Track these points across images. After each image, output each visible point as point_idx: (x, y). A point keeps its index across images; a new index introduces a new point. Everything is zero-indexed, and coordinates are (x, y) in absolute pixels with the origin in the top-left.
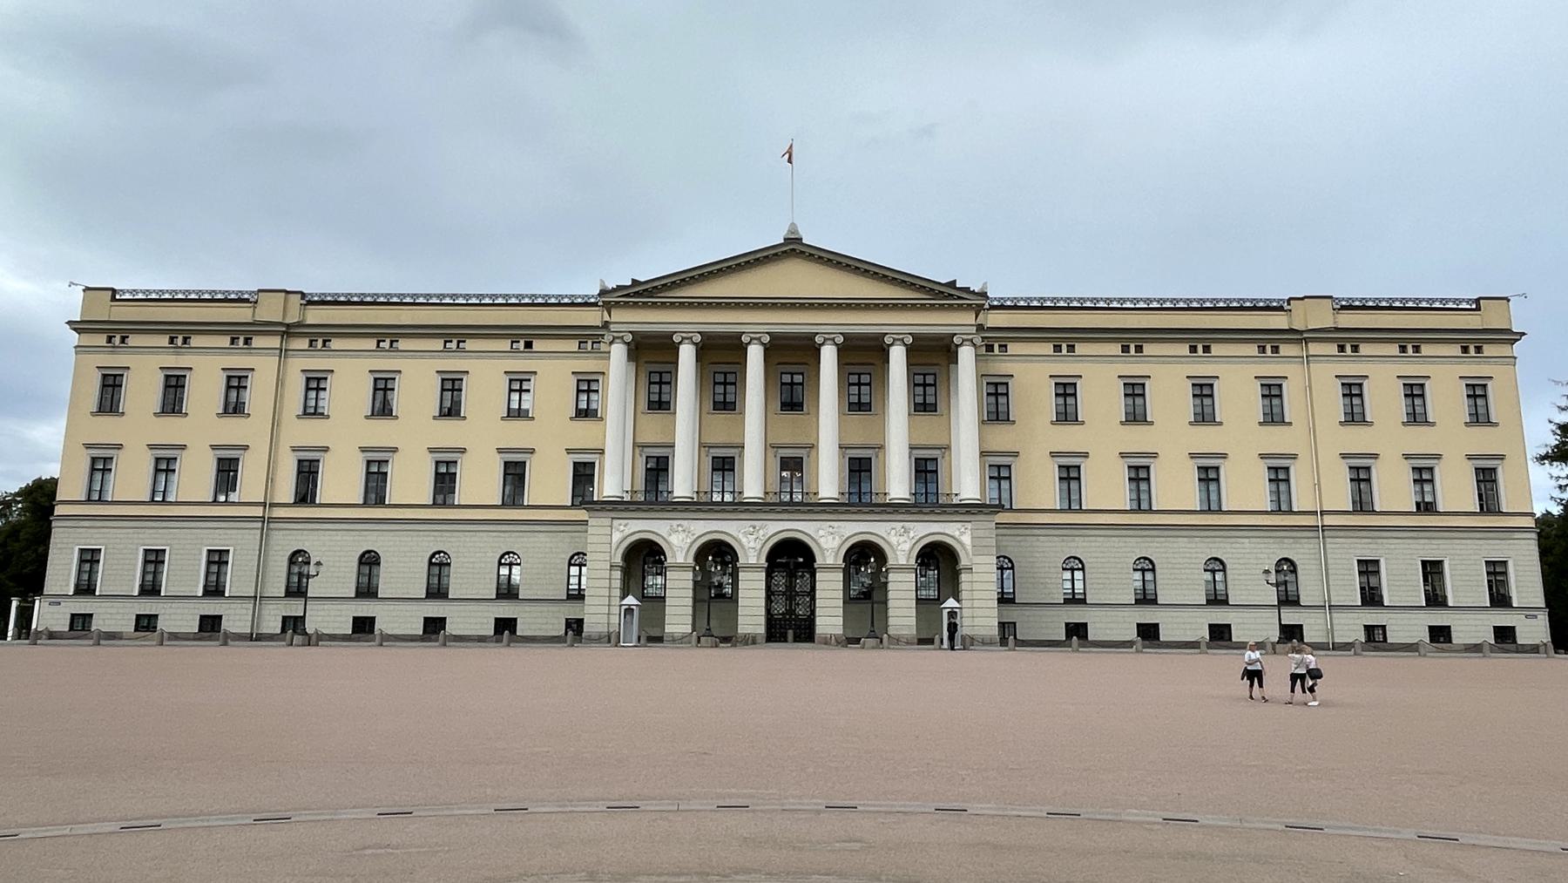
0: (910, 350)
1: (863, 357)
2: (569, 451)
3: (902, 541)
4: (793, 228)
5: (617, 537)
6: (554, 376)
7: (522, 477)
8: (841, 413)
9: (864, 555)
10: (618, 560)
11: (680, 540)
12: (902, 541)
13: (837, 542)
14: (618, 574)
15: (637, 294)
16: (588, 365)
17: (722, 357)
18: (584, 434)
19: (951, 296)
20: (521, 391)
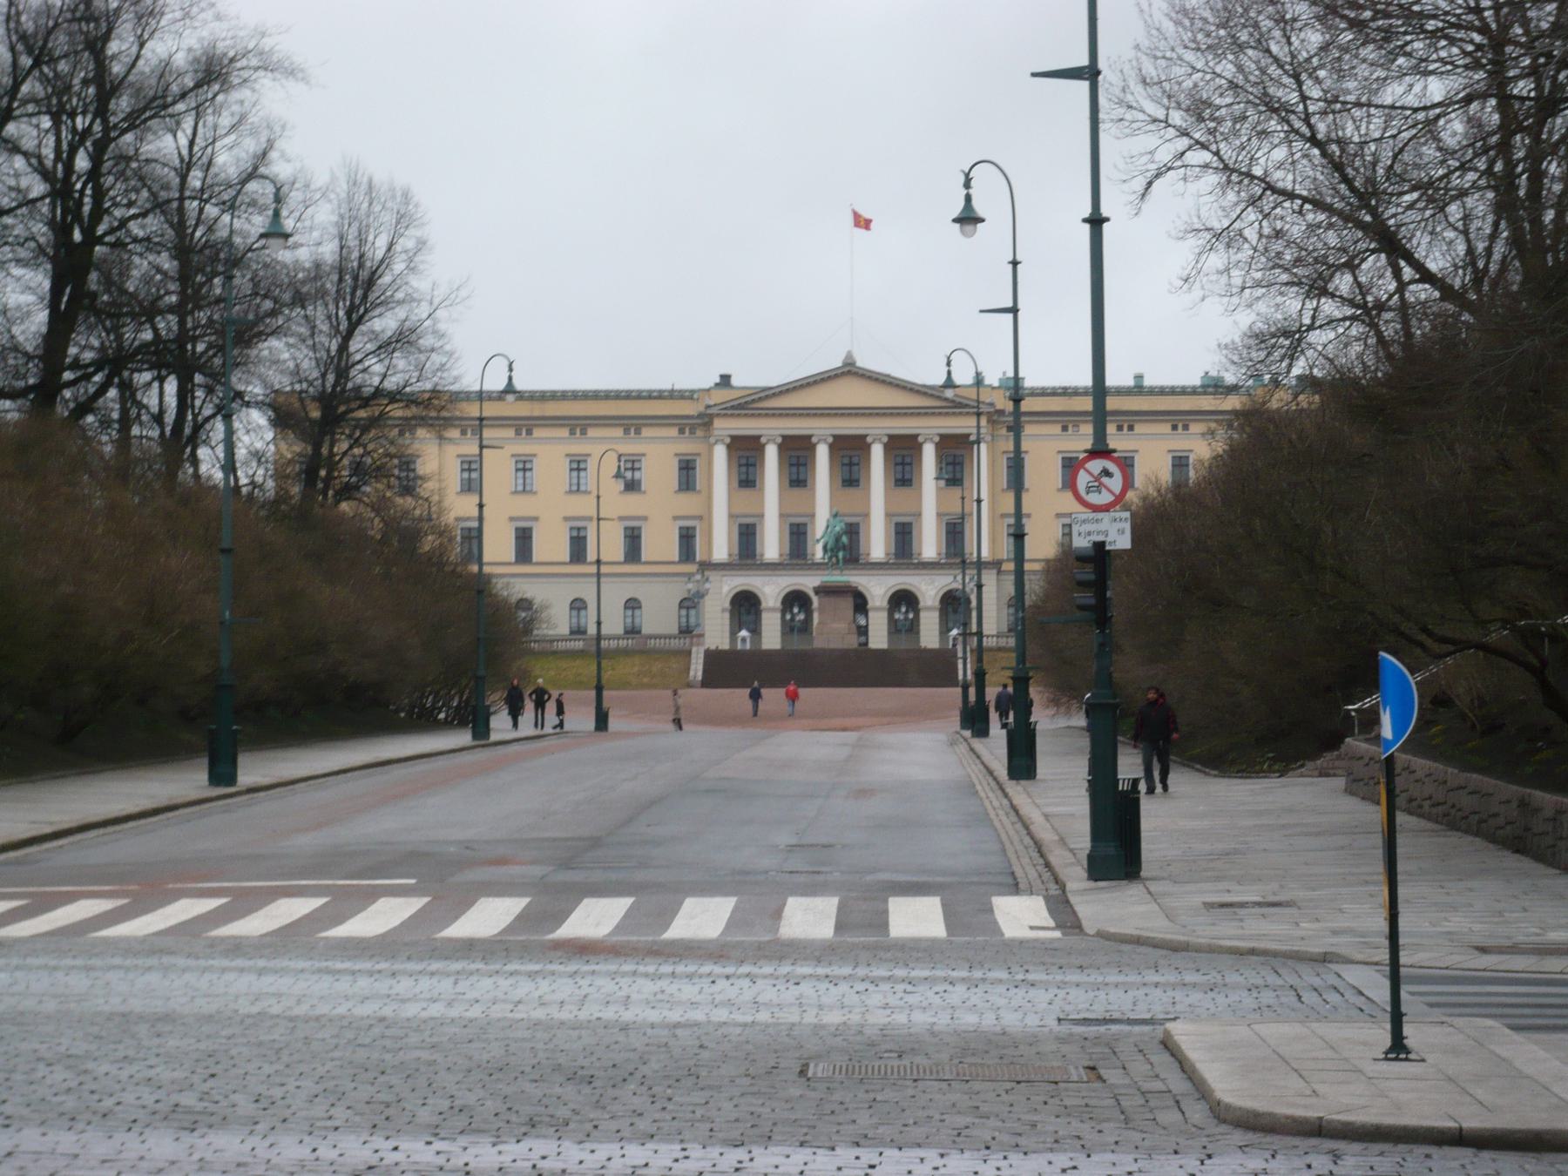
0: (937, 445)
1: (903, 452)
2: (676, 518)
3: (929, 589)
4: (849, 355)
5: (726, 589)
6: (659, 457)
7: (639, 537)
8: (886, 489)
9: (904, 599)
10: (727, 605)
11: (771, 590)
12: (929, 589)
13: (883, 591)
14: (727, 615)
15: (733, 407)
16: (687, 447)
17: (797, 453)
18: (688, 504)
19: (967, 406)
20: (633, 469)
